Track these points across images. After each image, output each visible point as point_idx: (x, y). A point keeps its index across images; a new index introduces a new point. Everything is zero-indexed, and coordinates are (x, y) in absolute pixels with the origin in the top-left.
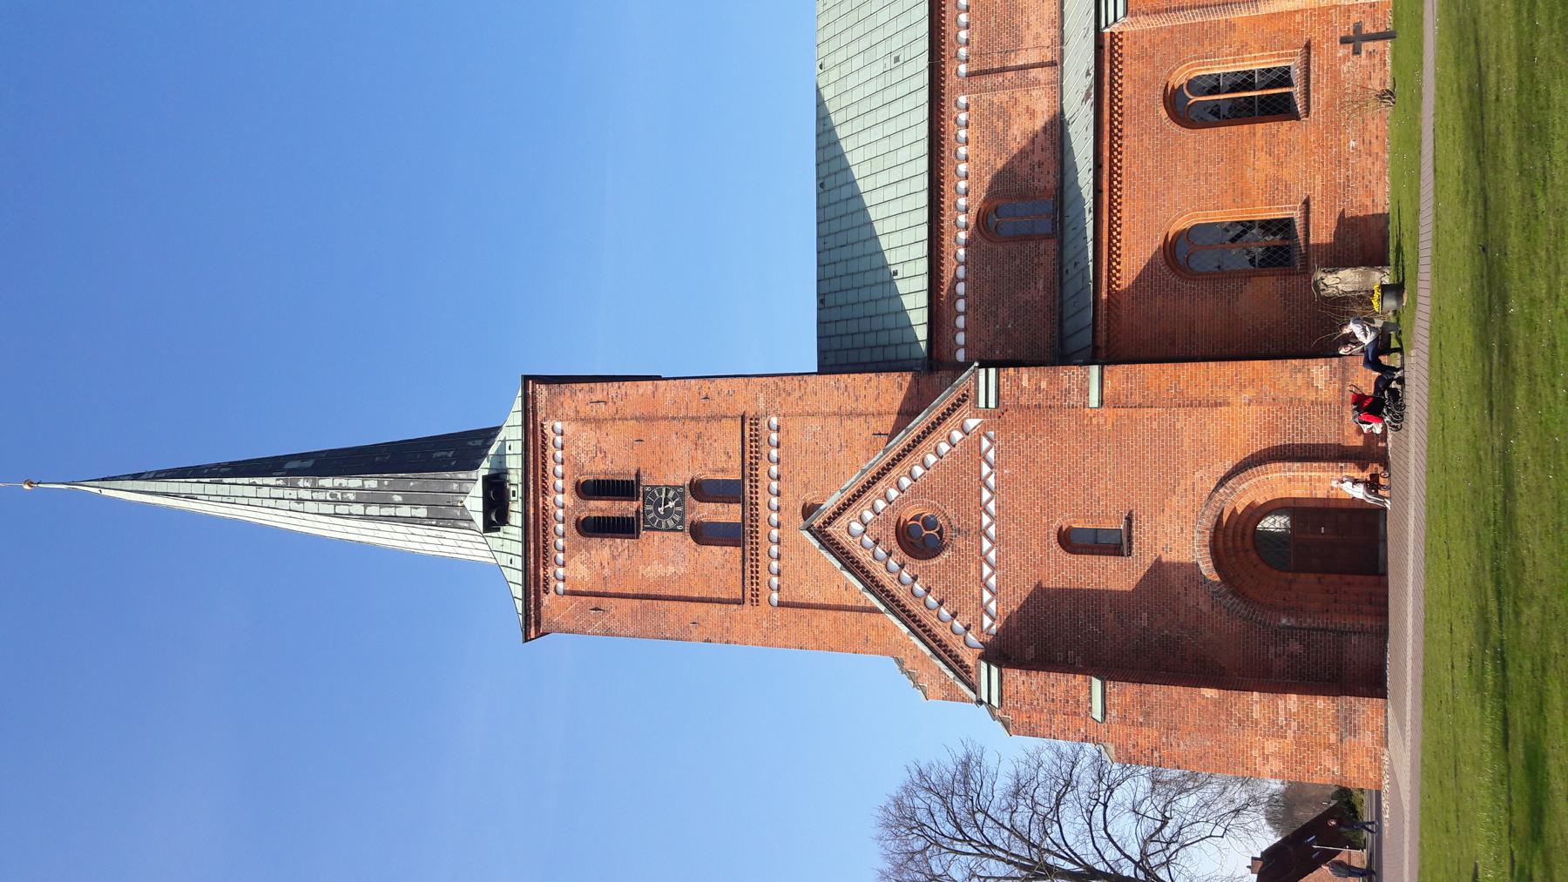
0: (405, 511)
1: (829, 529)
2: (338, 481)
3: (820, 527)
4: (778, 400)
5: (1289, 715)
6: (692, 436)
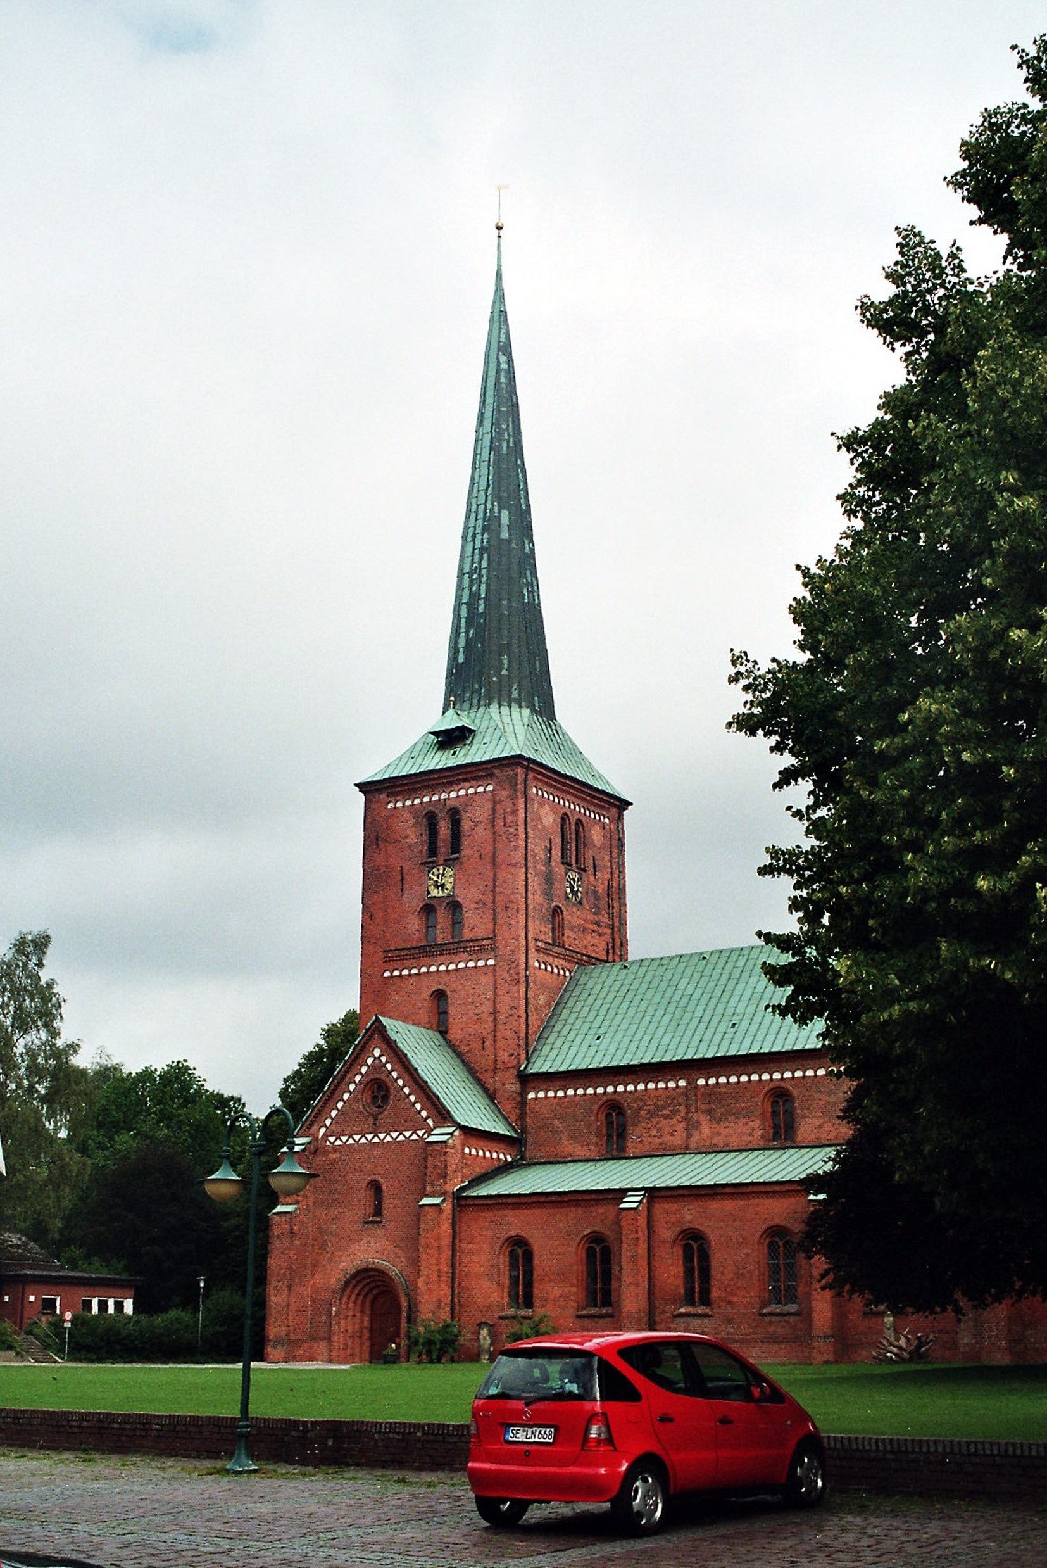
0: (462, 642)
2: (484, 572)
6: (484, 898)
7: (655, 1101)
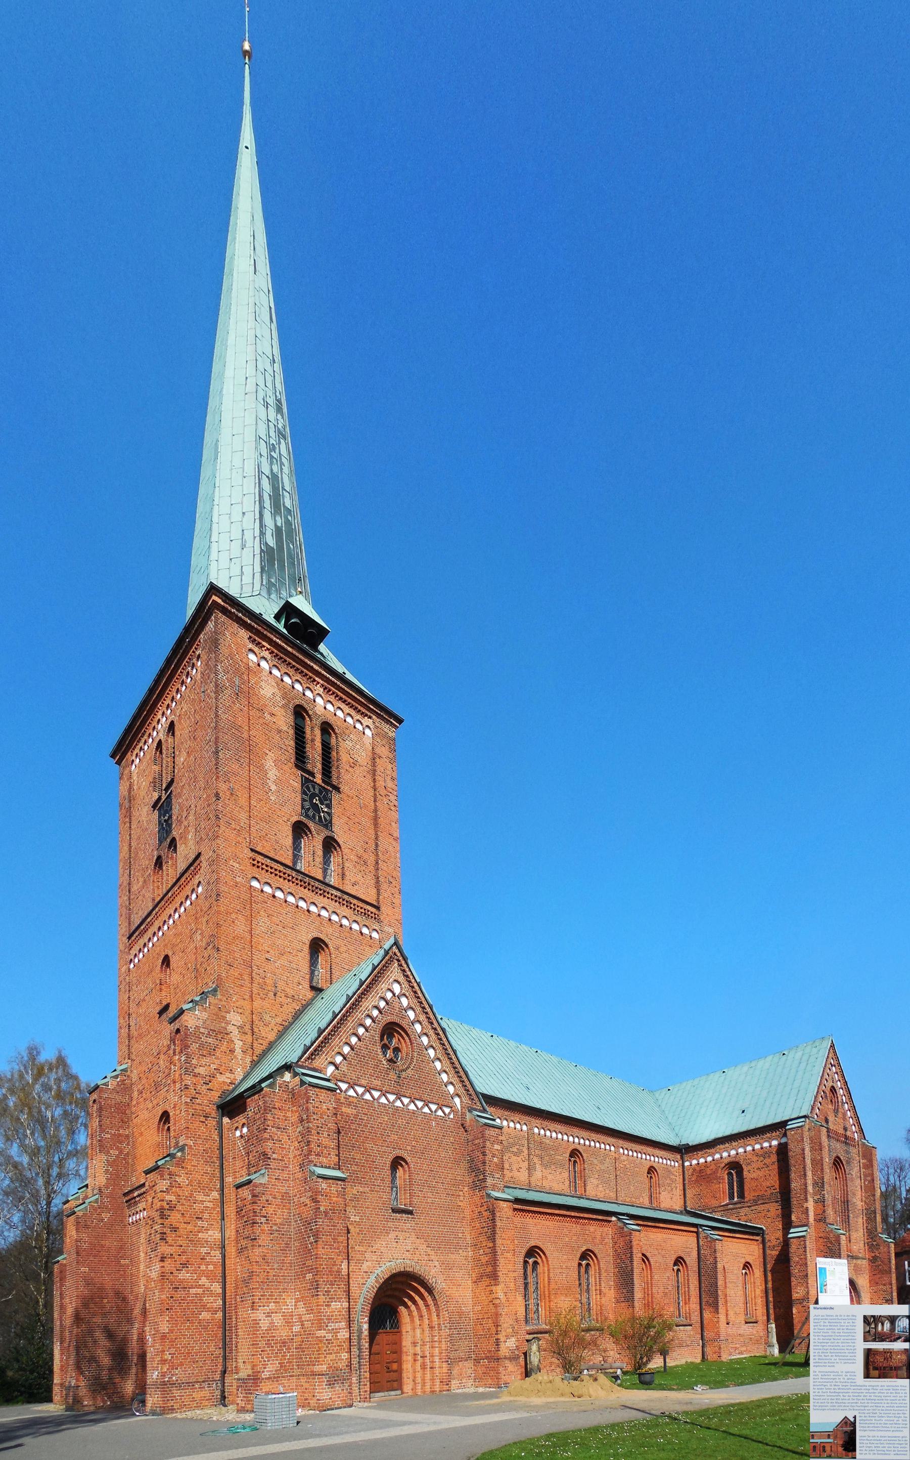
5: (335, 1332)
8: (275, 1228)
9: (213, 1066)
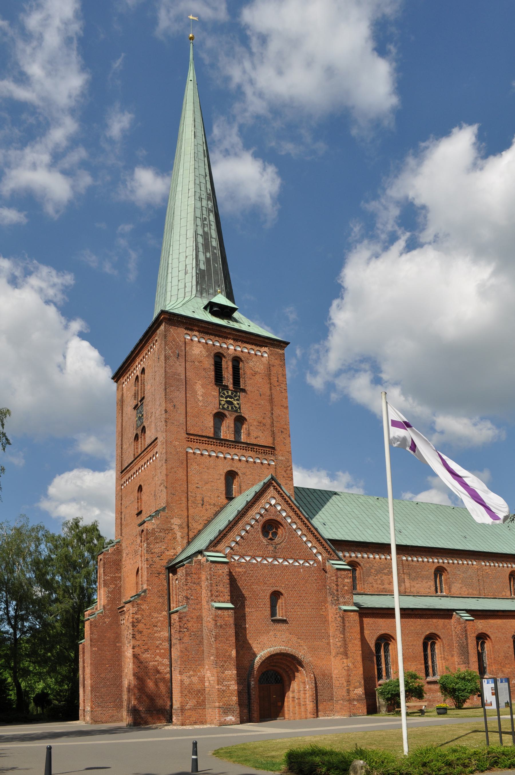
0: (202, 257)
1: (272, 488)
3: (272, 484)
4: (283, 466)
5: (228, 686)
7: (379, 564)
8: (192, 633)
9: (163, 547)
